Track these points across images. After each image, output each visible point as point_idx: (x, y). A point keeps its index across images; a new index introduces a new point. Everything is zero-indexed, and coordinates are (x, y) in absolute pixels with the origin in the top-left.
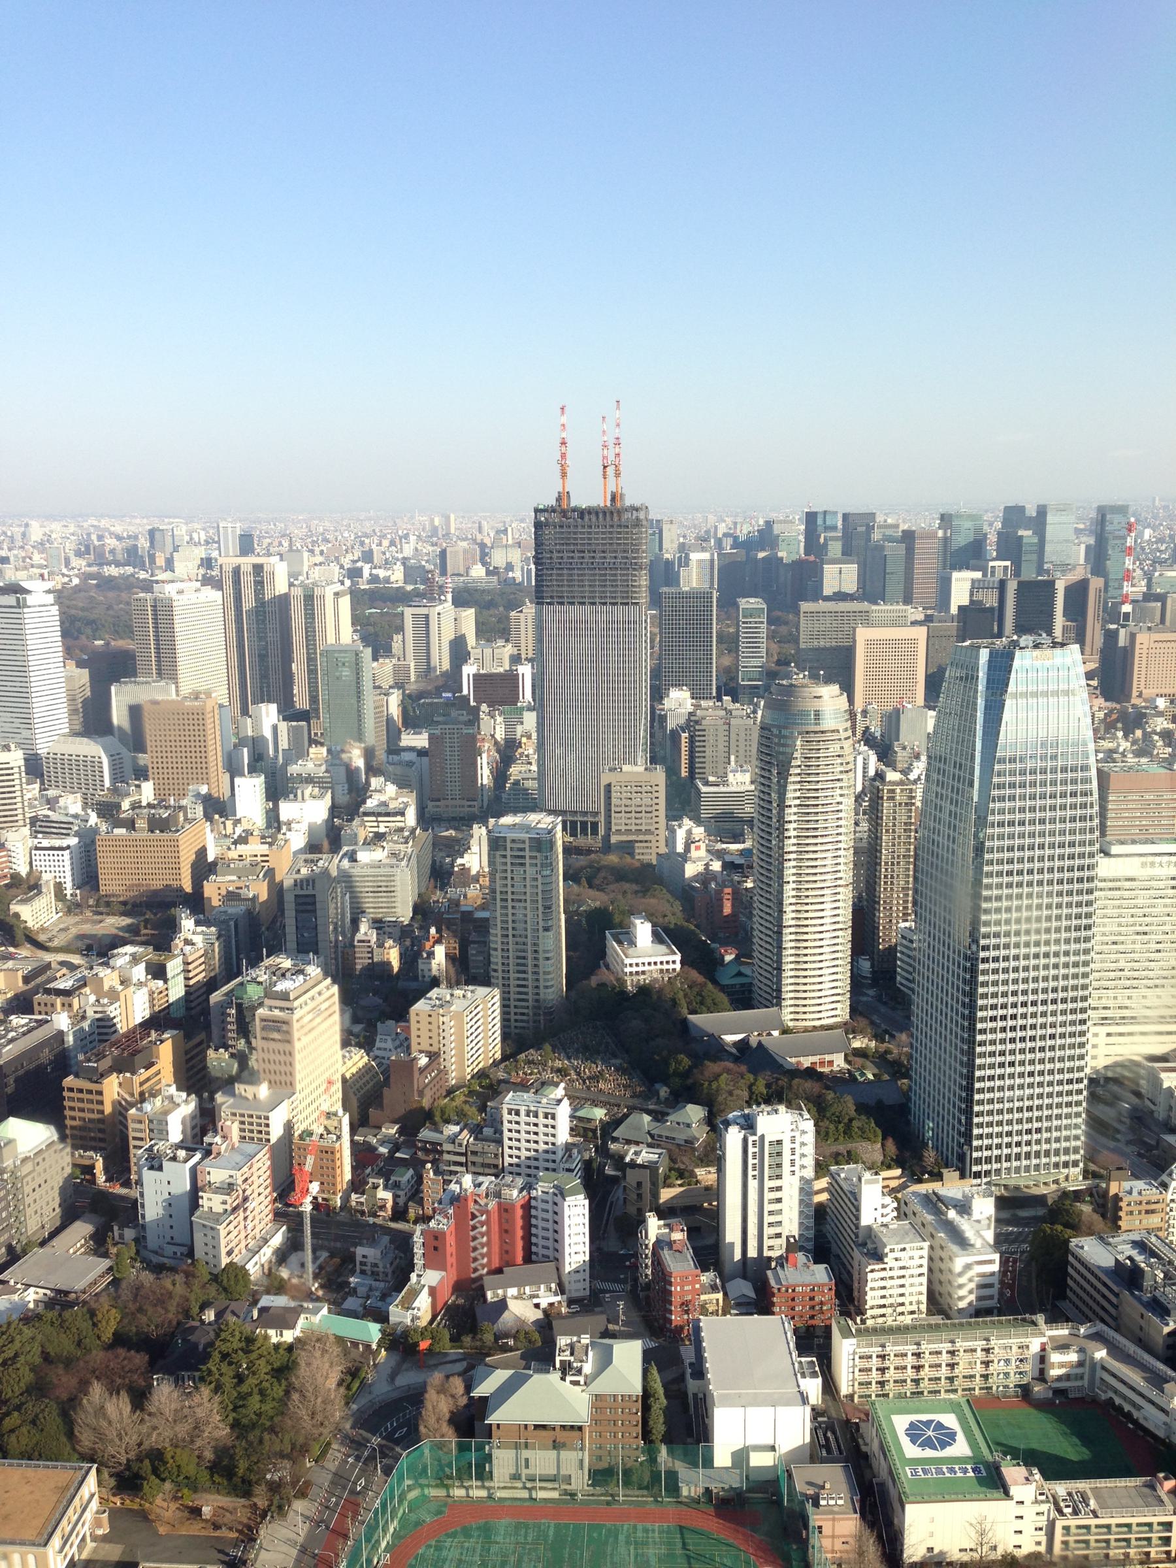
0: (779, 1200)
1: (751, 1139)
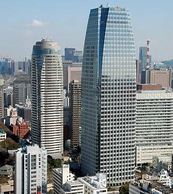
0: (35, 176)
1: (25, 155)
